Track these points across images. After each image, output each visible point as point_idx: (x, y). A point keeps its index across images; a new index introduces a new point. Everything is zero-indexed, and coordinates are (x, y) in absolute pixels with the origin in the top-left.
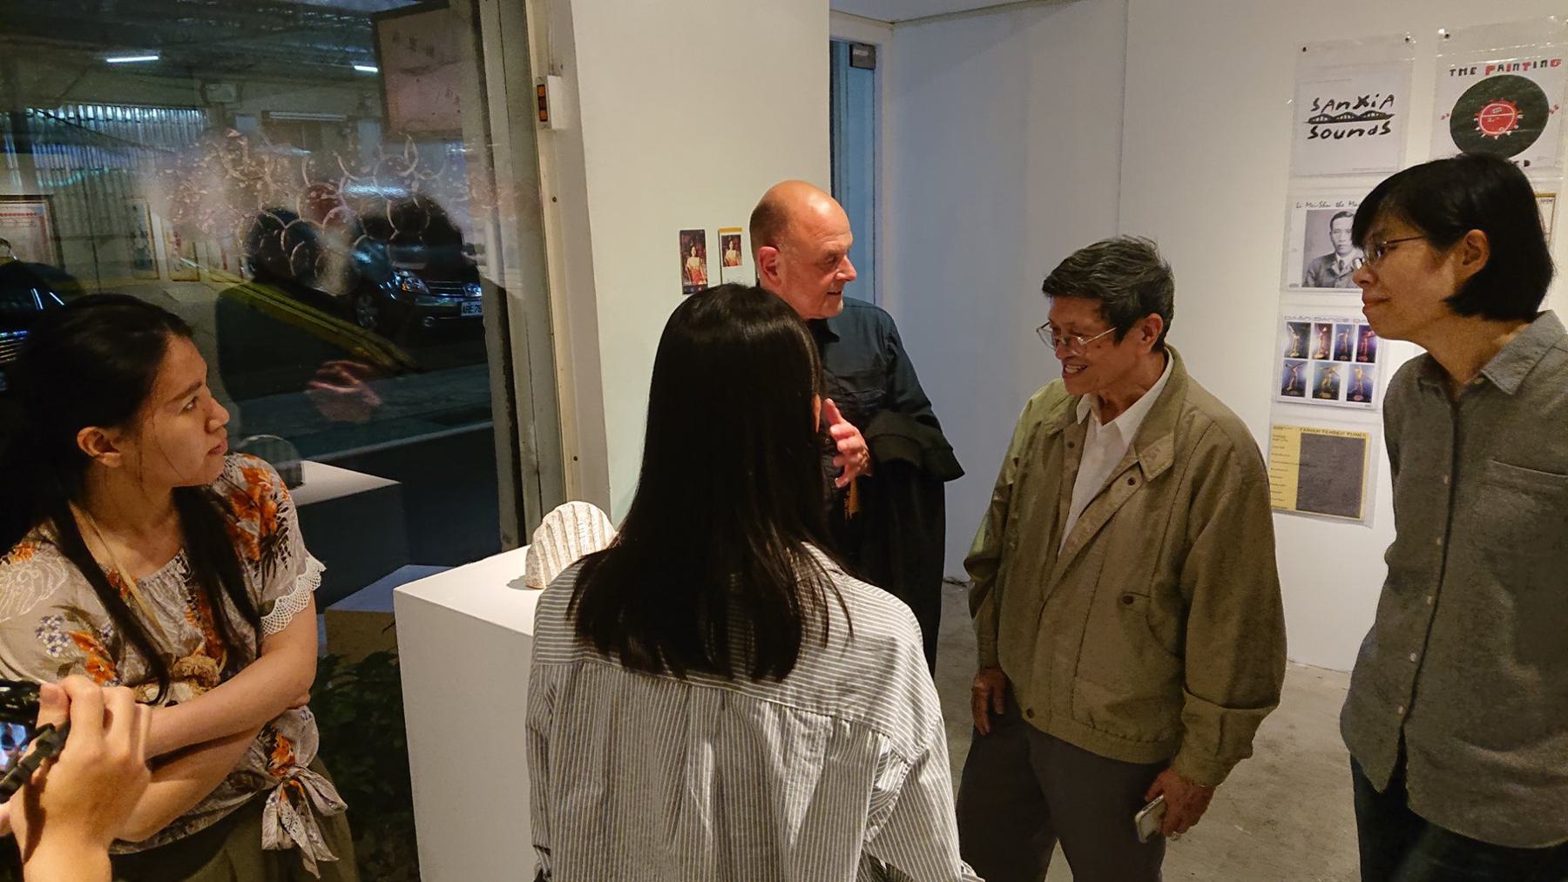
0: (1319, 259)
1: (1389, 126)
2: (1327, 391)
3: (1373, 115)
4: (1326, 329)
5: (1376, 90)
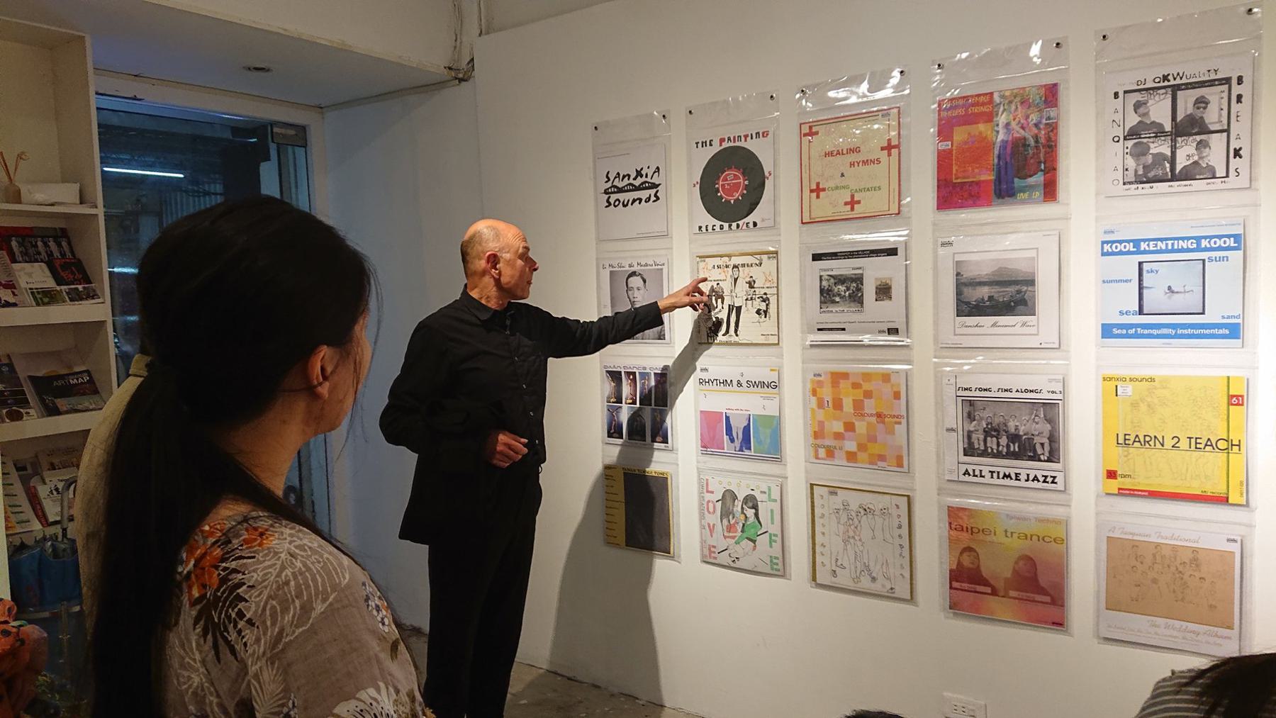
3: (647, 185)
4: (631, 375)
5: (647, 162)
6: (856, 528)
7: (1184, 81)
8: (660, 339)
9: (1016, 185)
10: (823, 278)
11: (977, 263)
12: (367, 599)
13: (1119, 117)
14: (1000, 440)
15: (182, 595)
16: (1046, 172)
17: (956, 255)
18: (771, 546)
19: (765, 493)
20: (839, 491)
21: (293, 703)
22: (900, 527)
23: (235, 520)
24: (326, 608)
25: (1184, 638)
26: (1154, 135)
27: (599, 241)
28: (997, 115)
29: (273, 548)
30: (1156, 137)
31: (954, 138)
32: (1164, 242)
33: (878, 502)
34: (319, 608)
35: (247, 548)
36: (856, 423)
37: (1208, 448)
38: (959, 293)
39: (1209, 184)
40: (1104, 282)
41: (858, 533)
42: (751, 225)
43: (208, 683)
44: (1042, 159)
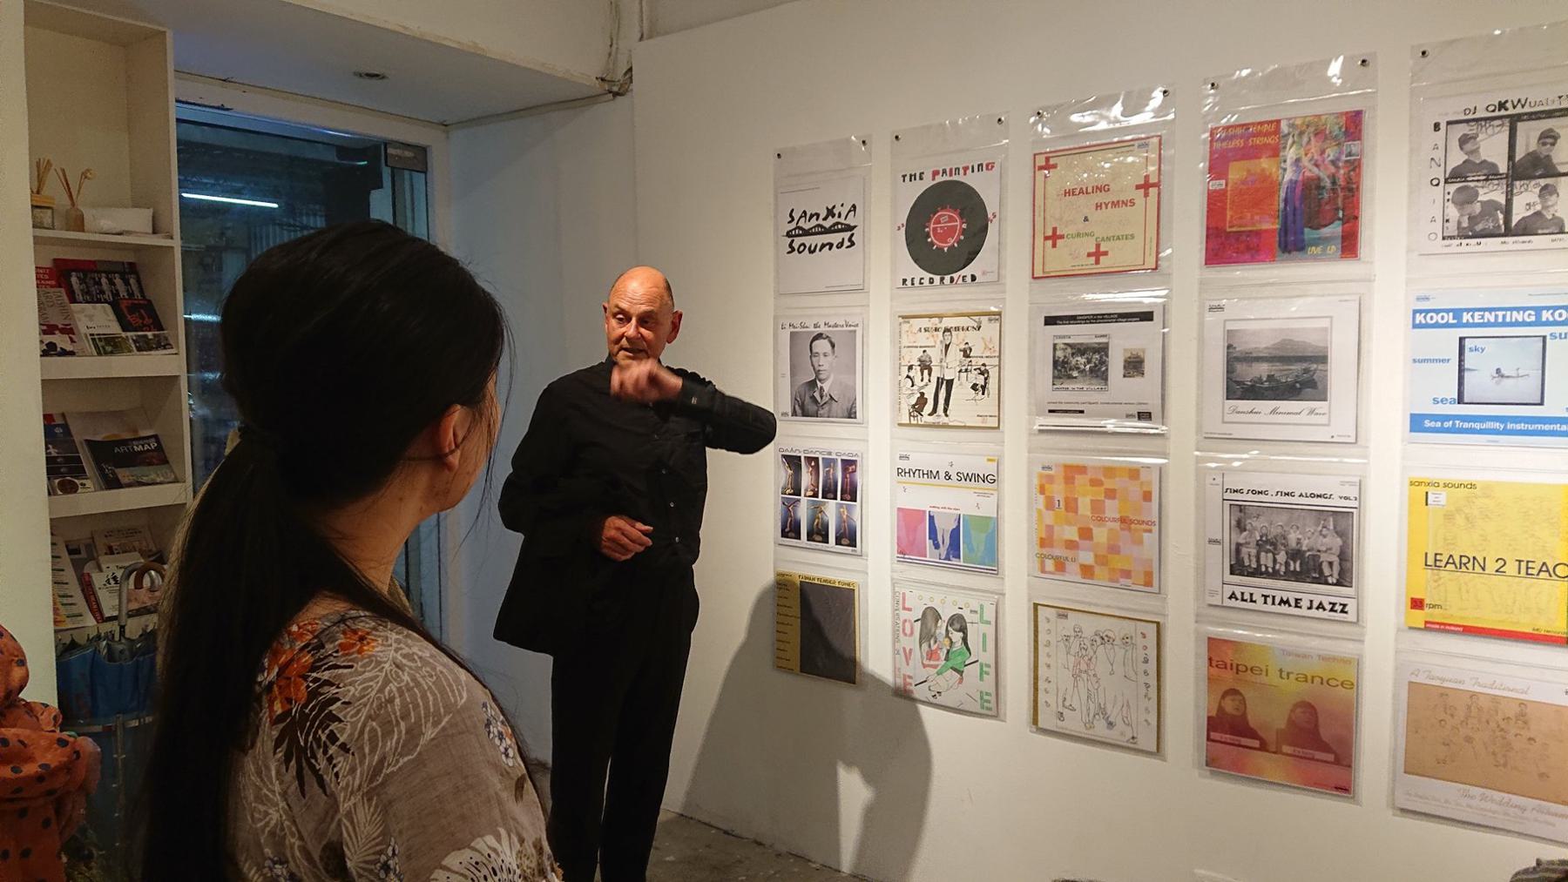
0: (803, 384)
1: (853, 239)
2: (819, 533)
3: (840, 226)
4: (813, 461)
5: (840, 199)
6: (1090, 660)
7: (1527, 109)
8: (850, 417)
9: (1306, 237)
10: (1058, 347)
11: (1255, 333)
12: (488, 724)
13: (1439, 155)
14: (1277, 557)
15: (261, 710)
16: (1345, 221)
17: (1227, 323)
18: (981, 679)
19: (976, 612)
20: (1070, 614)
21: (394, 850)
22: (1146, 661)
23: (328, 621)
24: (439, 733)
25: (1506, 814)
26: (1484, 178)
27: (779, 294)
28: (1285, 148)
29: (376, 657)
30: (1487, 180)
31: (1231, 176)
32: (1493, 313)
33: (1117, 629)
34: (429, 733)
35: (343, 655)
36: (1094, 532)
37: (1543, 575)
38: (1230, 371)
39: (1553, 241)
40: (1414, 361)
41: (1092, 667)
42: (969, 279)
43: (288, 820)
44: (1340, 204)
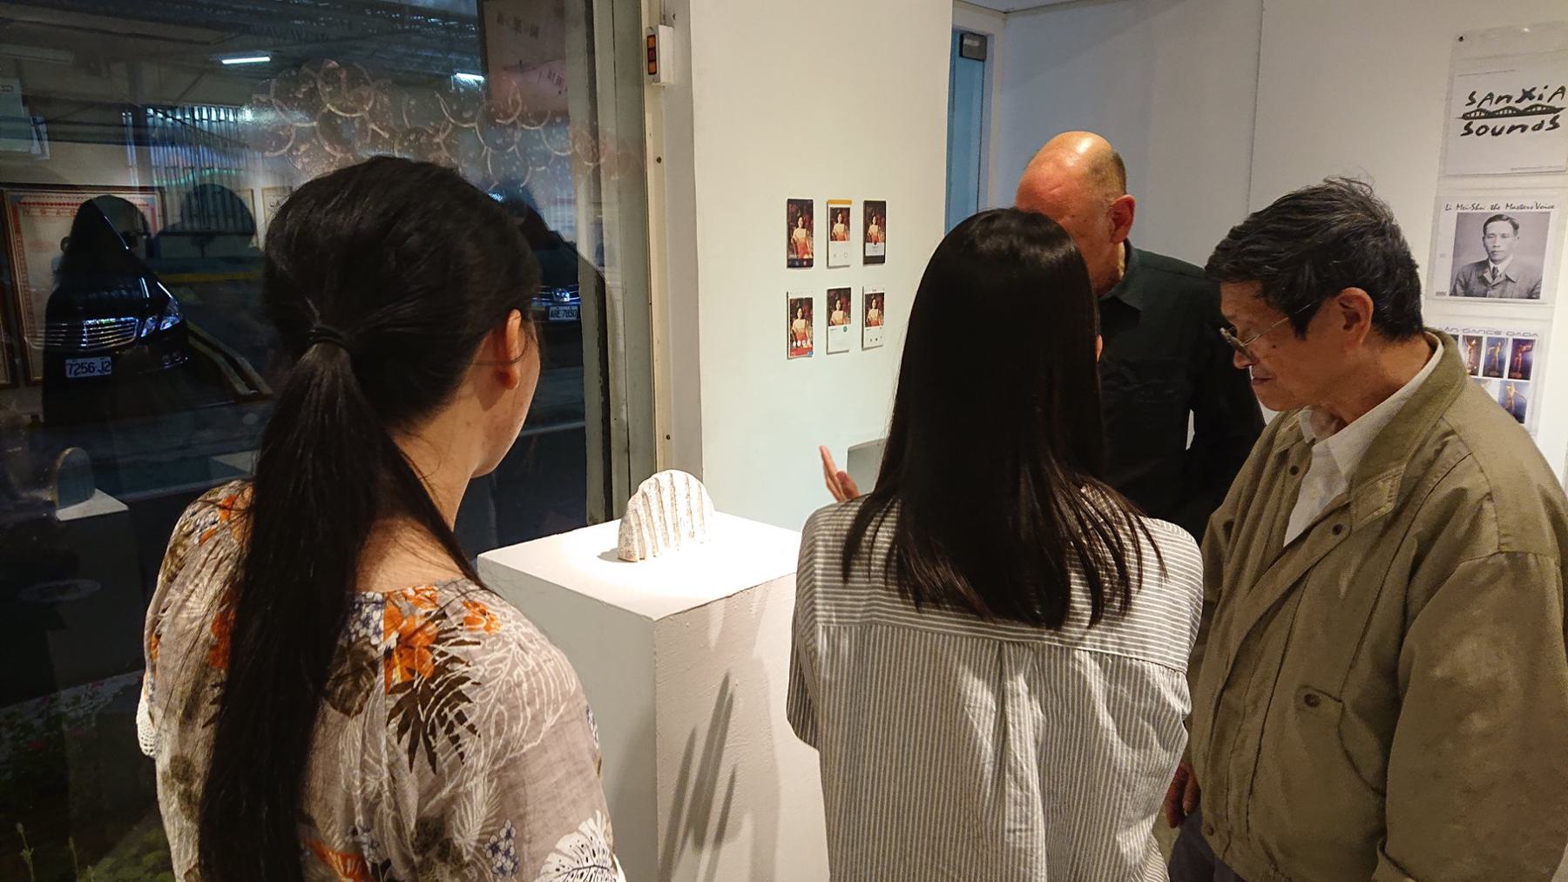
1: (1557, 121)
3: (1539, 109)
4: (1474, 342)
8: (1530, 297)
